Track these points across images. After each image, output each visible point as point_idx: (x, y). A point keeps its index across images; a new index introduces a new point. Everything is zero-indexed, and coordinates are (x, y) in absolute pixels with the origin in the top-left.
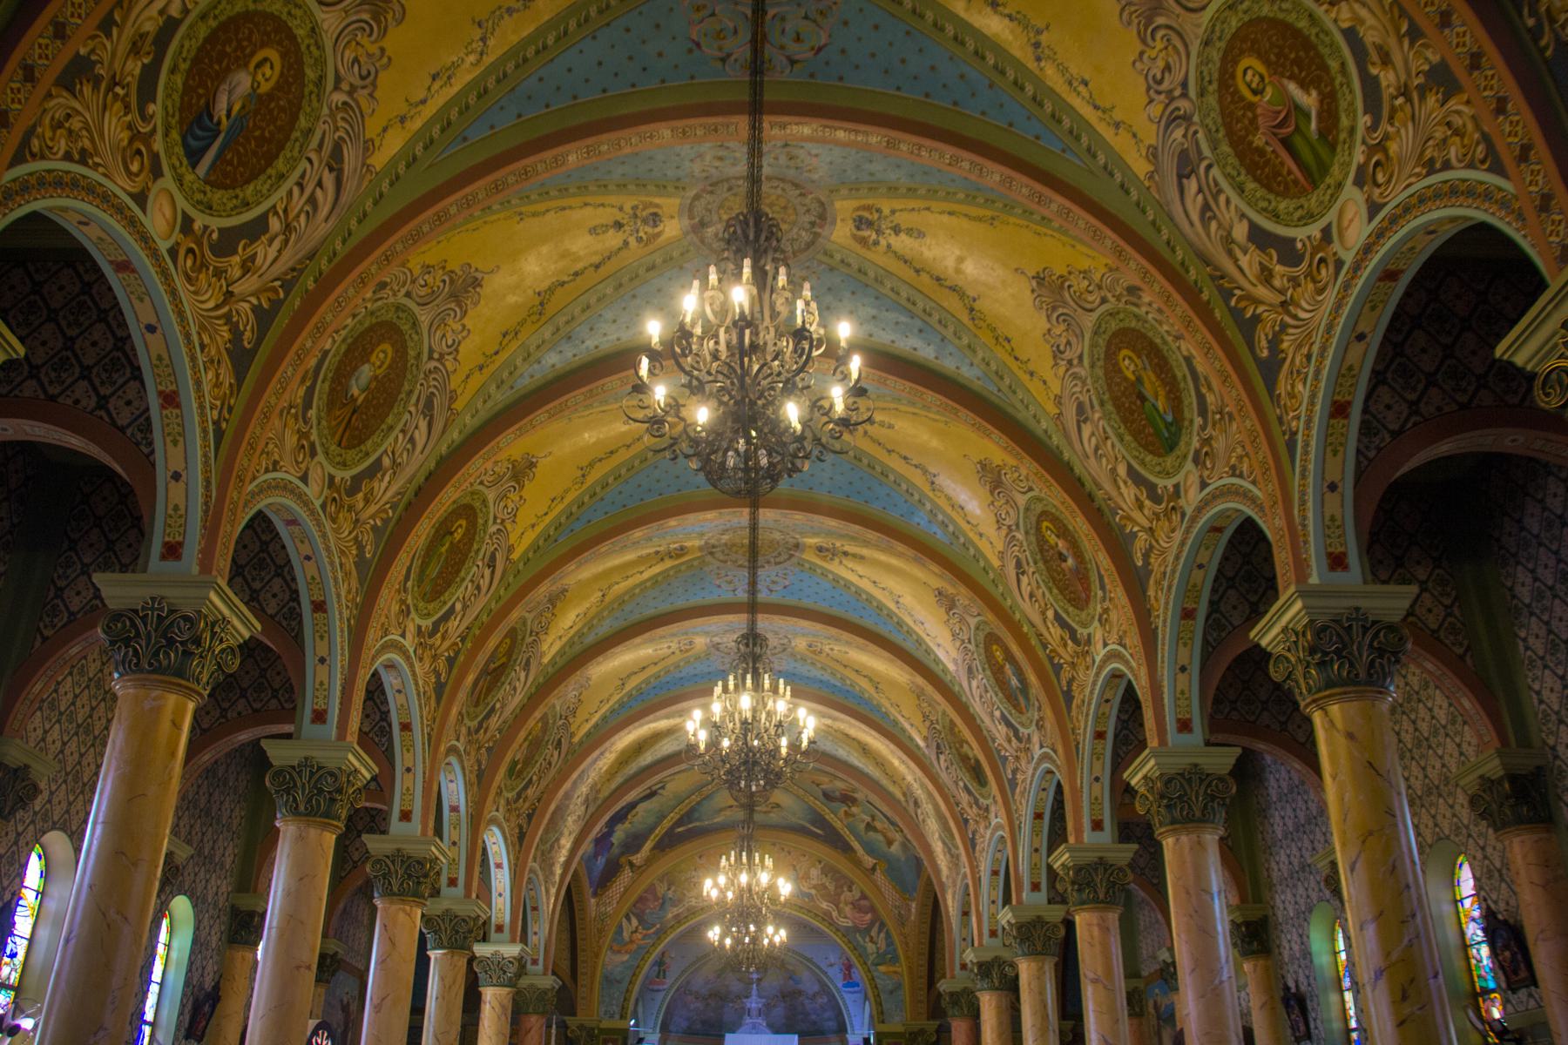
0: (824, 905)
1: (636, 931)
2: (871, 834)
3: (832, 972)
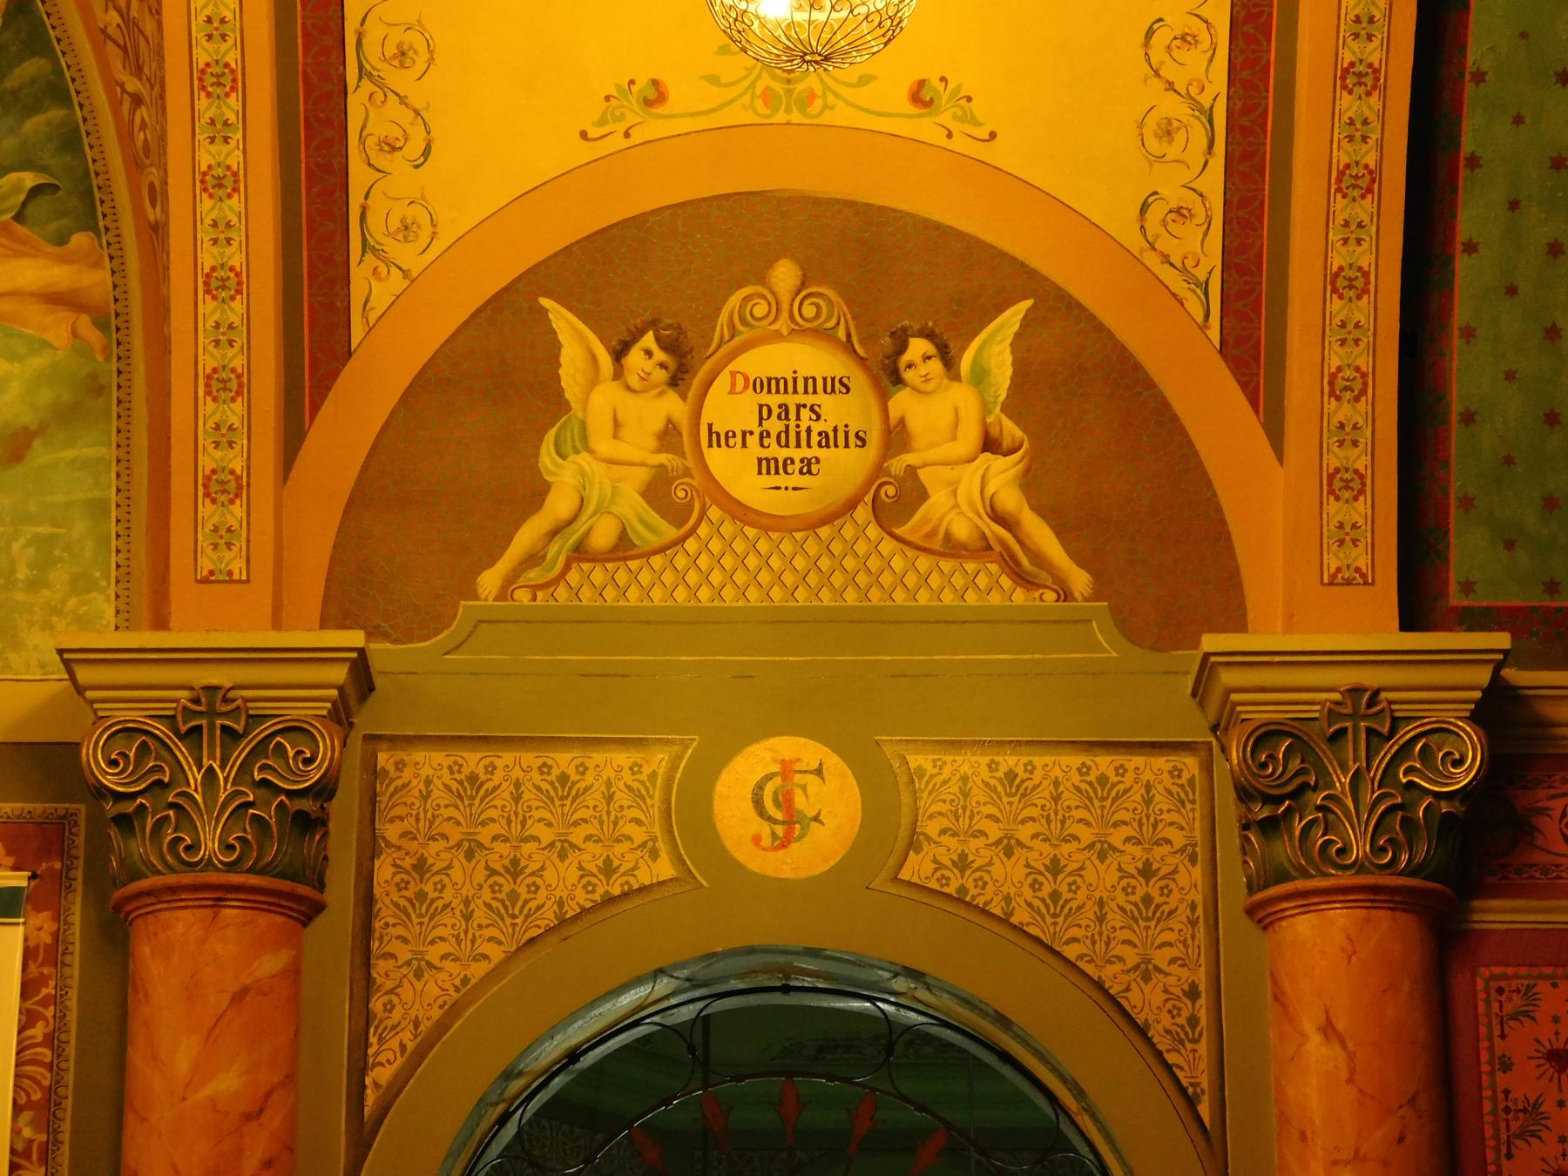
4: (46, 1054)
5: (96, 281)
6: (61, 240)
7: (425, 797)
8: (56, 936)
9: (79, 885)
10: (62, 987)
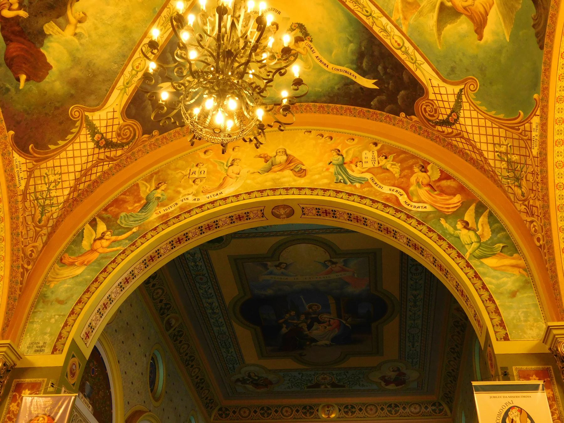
0: (386, 190)
1: (101, 238)
2: (449, 28)
6: (512, 255)
8: (553, 394)
9: (555, 383)
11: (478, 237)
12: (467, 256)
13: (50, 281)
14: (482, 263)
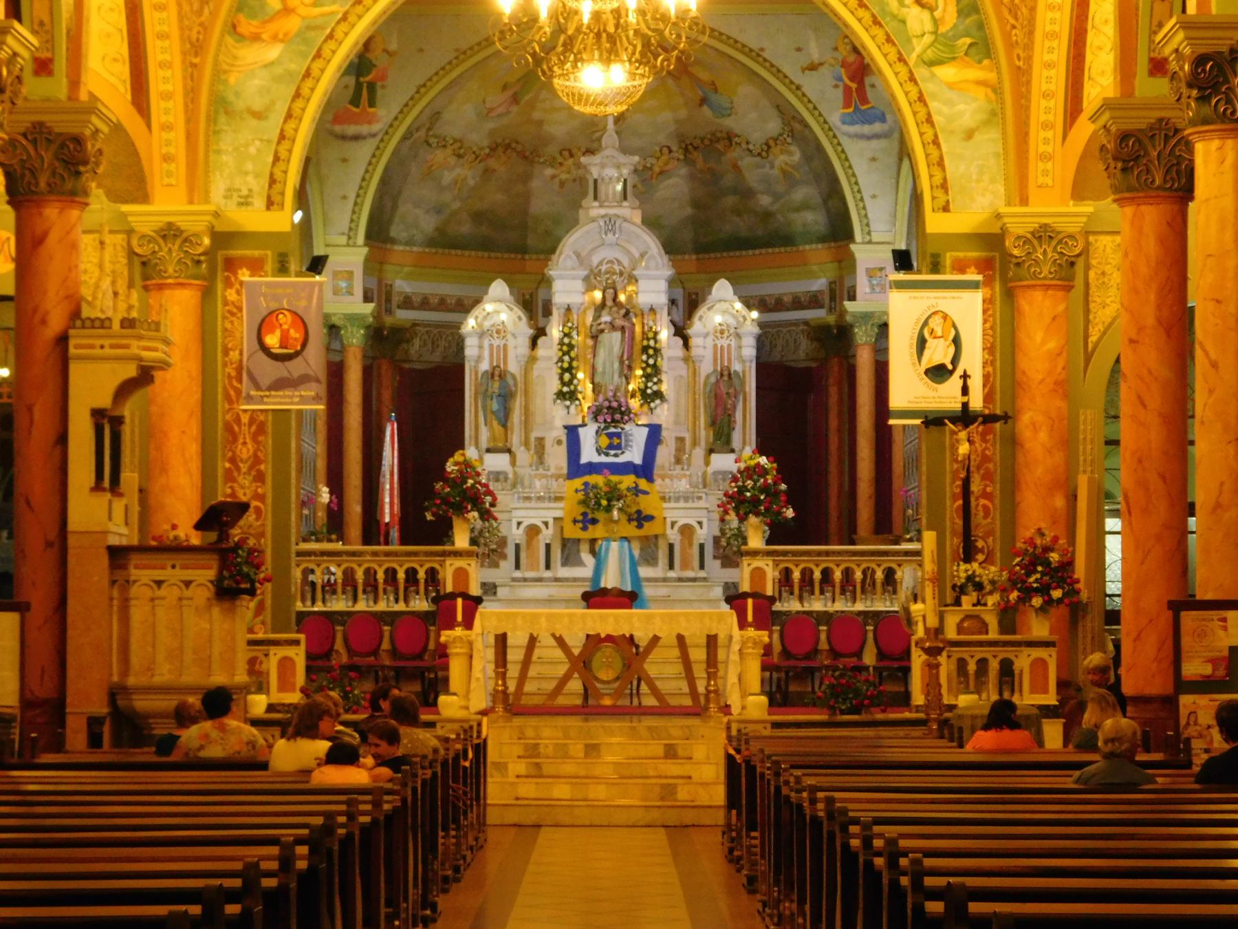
3: (810, 84)
4: (990, 332)
5: (992, 76)
6: (980, 62)
7: (1104, 251)
10: (994, 312)
11: (936, 22)
12: (912, 59)
13: (226, 72)
14: (933, 75)
